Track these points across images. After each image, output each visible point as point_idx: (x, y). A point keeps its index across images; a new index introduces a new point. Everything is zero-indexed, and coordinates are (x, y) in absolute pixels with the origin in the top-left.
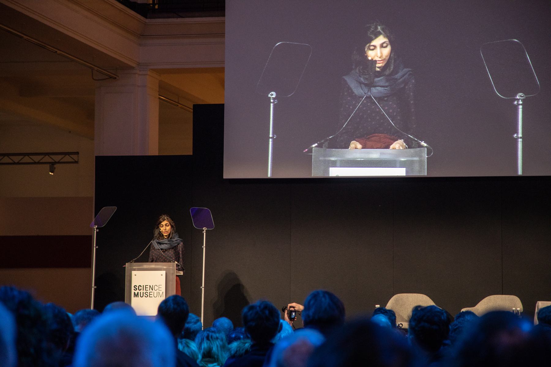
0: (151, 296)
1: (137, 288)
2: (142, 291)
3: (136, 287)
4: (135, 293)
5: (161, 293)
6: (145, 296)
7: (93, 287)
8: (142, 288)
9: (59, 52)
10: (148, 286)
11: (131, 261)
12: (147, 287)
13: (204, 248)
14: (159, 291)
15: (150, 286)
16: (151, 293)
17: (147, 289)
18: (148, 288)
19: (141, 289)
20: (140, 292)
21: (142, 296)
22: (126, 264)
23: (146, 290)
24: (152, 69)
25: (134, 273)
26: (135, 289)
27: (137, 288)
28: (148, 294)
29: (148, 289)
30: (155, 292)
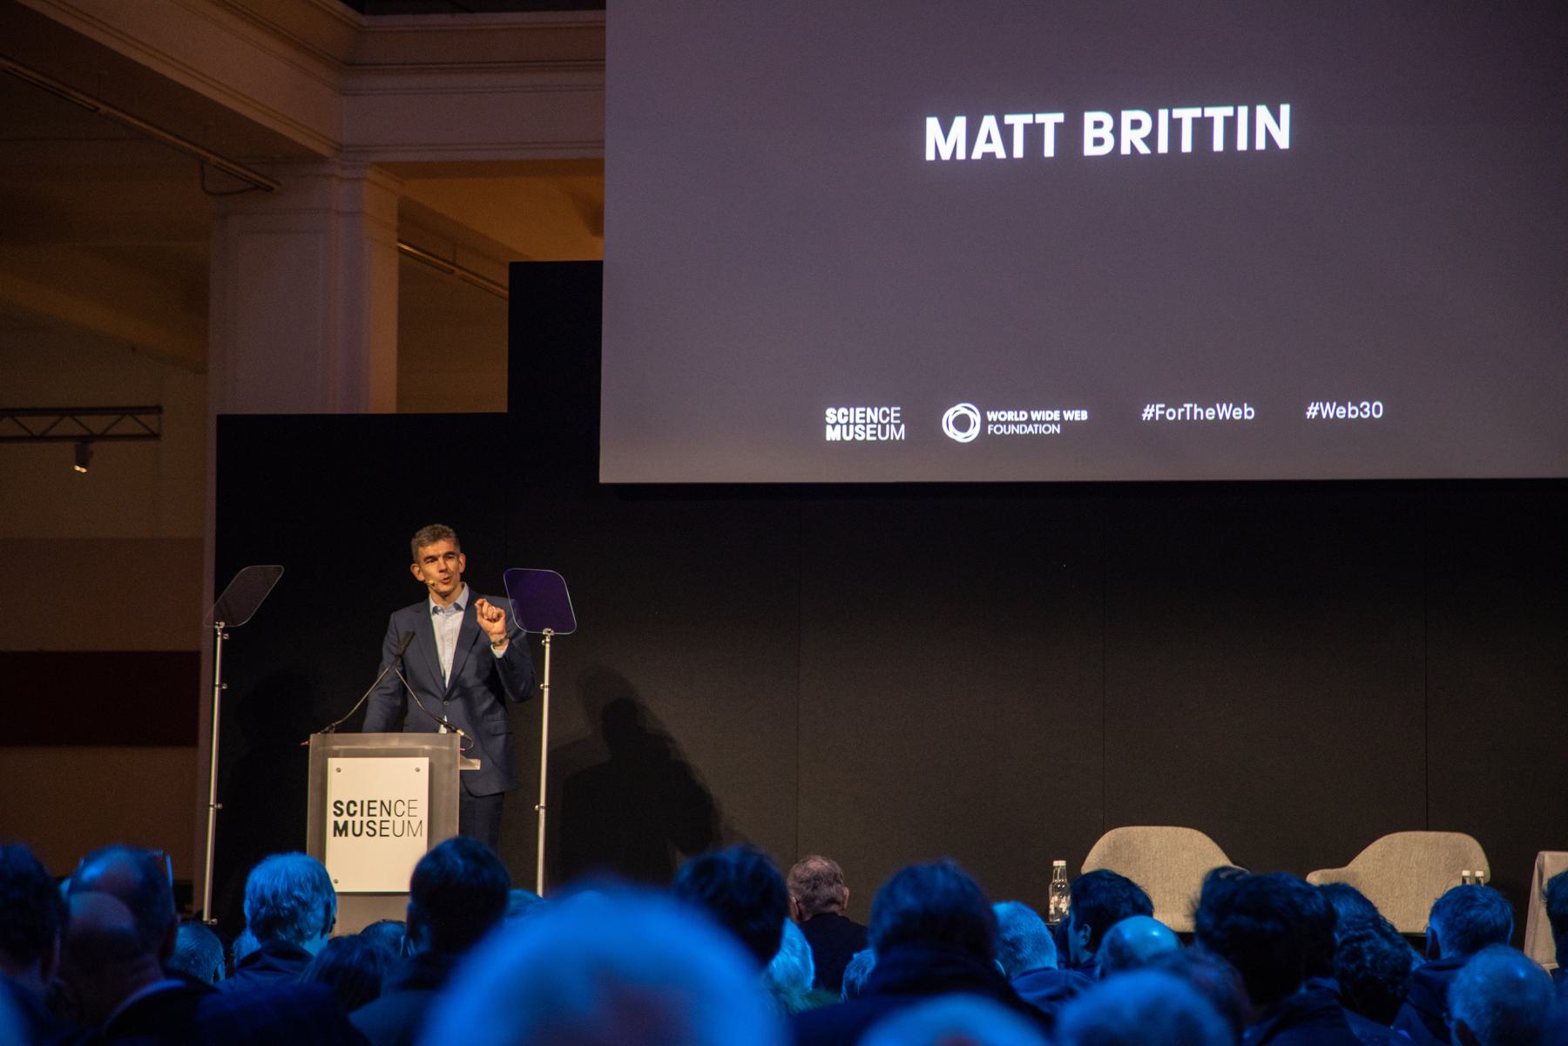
0: (384, 832)
1: (344, 808)
2: (357, 818)
3: (341, 807)
4: (336, 823)
5: (415, 824)
6: (367, 833)
7: (213, 806)
8: (358, 809)
9: (104, 109)
10: (375, 801)
11: (327, 729)
12: (372, 805)
13: (546, 690)
14: (410, 819)
15: (382, 803)
16: (384, 825)
17: (372, 812)
18: (375, 808)
19: (355, 812)
20: (354, 822)
21: (357, 832)
22: (312, 736)
23: (369, 815)
24: (381, 165)
25: (333, 763)
26: (339, 812)
27: (344, 808)
28: (377, 828)
29: (377, 812)
30: (399, 821)
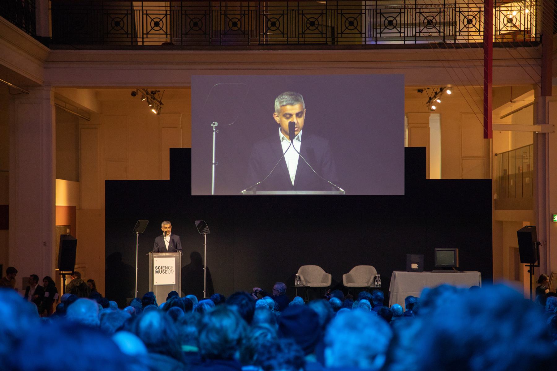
0: (166, 273)
1: (158, 268)
2: (160, 270)
4: (156, 271)
5: (173, 271)
8: (161, 268)
16: (166, 271)
17: (164, 269)
21: (161, 273)
27: (158, 268)
30: (169, 270)
